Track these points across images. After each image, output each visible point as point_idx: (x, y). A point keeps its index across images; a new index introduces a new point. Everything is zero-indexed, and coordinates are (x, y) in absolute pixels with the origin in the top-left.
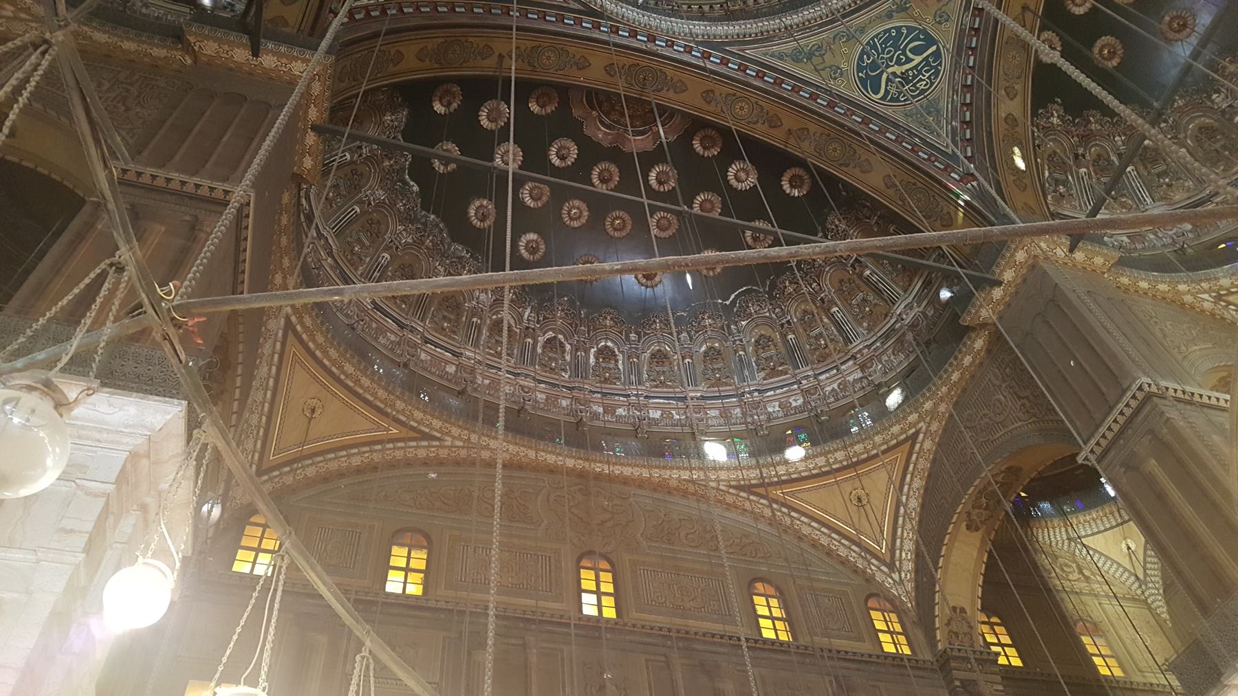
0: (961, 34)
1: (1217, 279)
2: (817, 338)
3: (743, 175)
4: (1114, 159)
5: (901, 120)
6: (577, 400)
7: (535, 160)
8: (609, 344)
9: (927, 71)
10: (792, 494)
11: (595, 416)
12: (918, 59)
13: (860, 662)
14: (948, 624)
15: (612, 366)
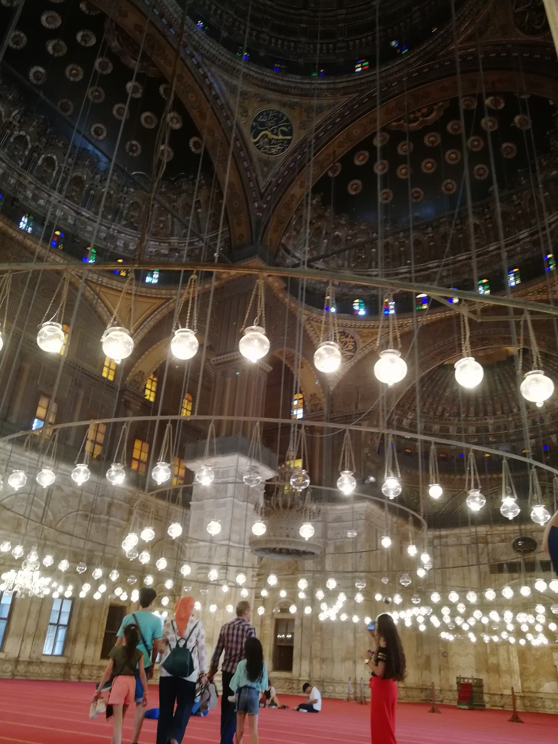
0: (304, 141)
1: (313, 313)
2: (161, 222)
3: (175, 121)
4: (324, 232)
5: (255, 160)
6: (20, 184)
7: (66, 33)
8: (55, 157)
9: (280, 146)
10: (103, 292)
11: (26, 198)
12: (281, 137)
13: (89, 376)
14: (134, 376)
15: (49, 171)
